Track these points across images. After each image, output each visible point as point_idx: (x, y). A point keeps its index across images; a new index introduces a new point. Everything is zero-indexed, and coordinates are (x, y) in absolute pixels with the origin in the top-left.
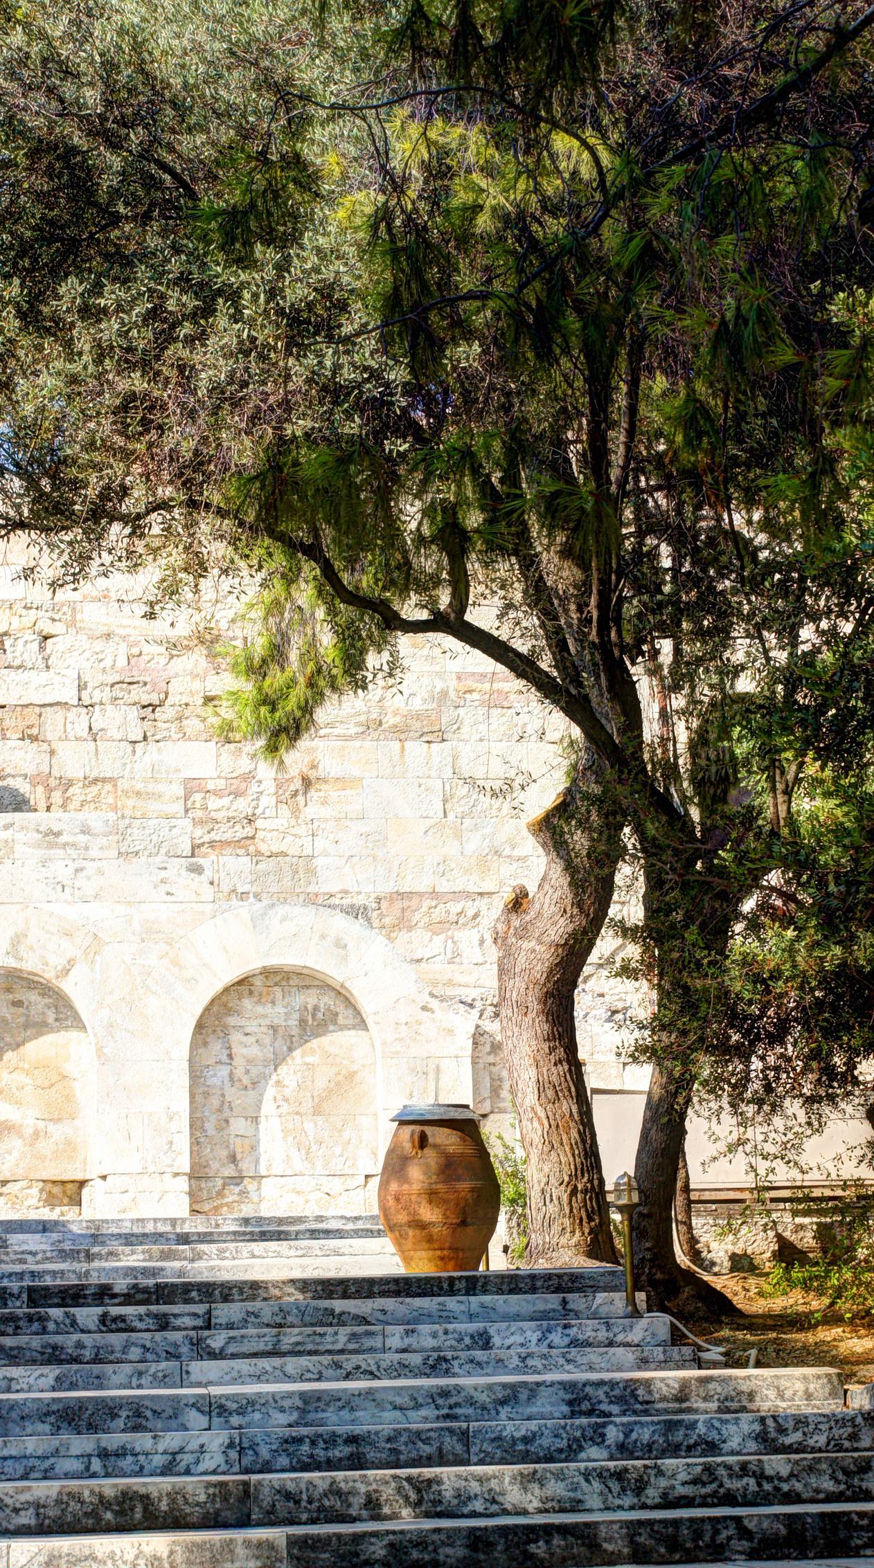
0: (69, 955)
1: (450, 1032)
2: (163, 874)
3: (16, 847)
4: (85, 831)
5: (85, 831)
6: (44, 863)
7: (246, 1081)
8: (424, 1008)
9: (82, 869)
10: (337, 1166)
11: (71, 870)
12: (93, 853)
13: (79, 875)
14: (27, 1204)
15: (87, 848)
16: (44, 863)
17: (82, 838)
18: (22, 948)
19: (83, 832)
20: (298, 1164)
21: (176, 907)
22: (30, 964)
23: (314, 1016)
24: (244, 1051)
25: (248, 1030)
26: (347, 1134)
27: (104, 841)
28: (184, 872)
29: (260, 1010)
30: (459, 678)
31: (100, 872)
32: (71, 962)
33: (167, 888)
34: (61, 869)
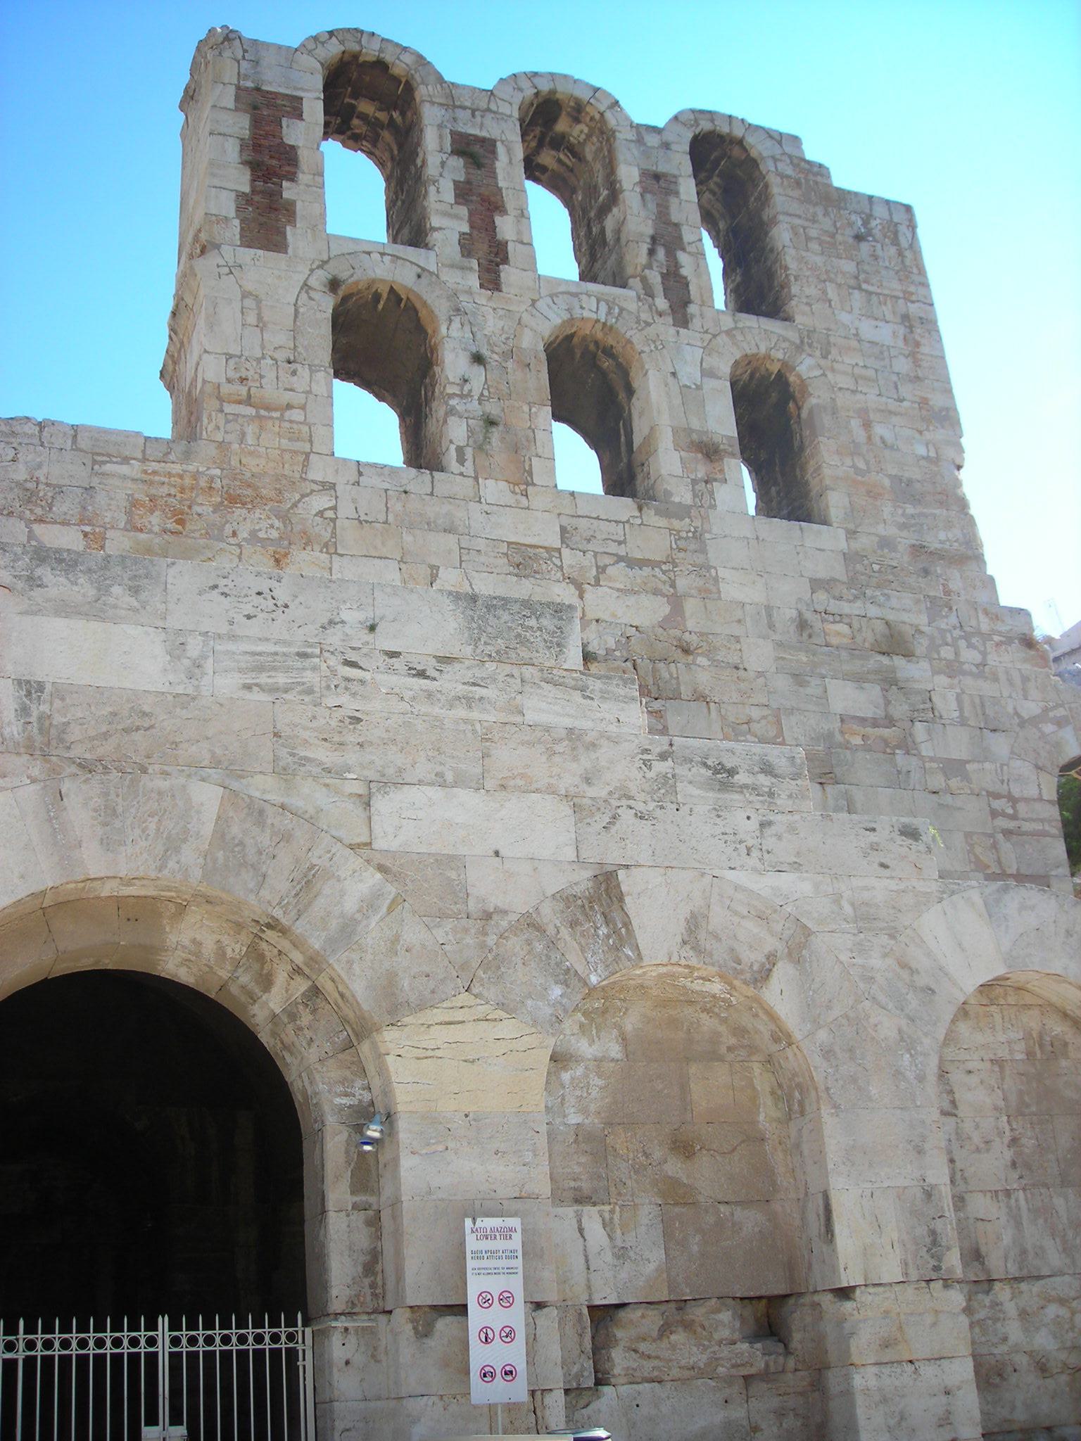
0: (768, 949)
2: (872, 837)
4: (767, 769)
5: (767, 769)
6: (718, 811)
9: (770, 823)
11: (753, 825)
12: (783, 801)
13: (768, 831)
16: (718, 811)
17: (764, 780)
18: (702, 935)
19: (763, 771)
21: (893, 885)
23: (1041, 1046)
25: (970, 1066)
28: (896, 835)
29: (980, 1038)
30: (842, 721)
31: (792, 829)
32: (772, 959)
33: (877, 857)
34: (742, 820)
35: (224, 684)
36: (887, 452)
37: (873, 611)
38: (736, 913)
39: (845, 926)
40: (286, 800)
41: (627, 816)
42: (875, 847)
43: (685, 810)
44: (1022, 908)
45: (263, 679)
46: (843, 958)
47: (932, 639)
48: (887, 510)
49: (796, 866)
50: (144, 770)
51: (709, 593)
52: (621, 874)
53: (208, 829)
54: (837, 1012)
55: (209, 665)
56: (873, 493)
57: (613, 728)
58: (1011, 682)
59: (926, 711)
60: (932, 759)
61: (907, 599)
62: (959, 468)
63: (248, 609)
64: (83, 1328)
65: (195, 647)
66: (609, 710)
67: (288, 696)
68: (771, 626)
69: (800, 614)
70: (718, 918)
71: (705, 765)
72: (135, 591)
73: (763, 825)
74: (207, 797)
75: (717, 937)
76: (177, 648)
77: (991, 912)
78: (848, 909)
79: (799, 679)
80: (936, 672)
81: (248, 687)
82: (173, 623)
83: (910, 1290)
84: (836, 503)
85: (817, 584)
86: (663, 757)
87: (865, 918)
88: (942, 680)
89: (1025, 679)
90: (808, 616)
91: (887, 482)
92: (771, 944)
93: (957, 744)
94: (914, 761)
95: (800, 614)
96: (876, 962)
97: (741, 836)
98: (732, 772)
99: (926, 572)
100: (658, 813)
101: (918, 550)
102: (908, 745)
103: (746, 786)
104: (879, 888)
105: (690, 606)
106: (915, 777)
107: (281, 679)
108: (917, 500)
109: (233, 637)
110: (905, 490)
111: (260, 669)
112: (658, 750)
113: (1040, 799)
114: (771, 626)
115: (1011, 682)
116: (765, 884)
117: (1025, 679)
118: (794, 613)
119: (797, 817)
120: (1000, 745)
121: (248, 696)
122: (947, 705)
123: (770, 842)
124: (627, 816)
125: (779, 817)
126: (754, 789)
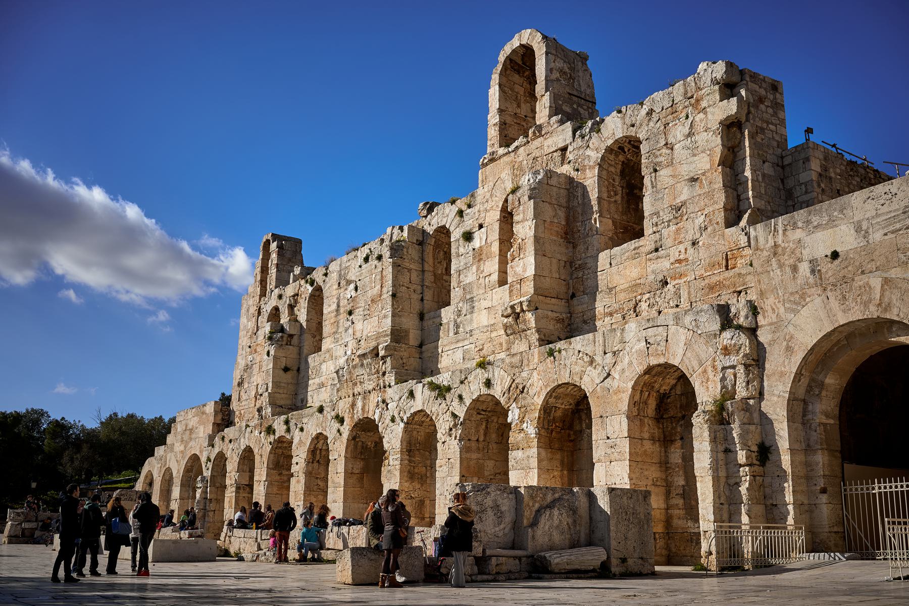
35: (877, 236)
40: (905, 276)
45: (891, 228)
50: (853, 280)
53: (878, 297)
55: (870, 231)
63: (883, 201)
64: (862, 484)
65: (865, 226)
67: (901, 232)
72: (841, 211)
74: (876, 282)
76: (858, 229)
81: (886, 234)
82: (856, 219)
107: (898, 226)
109: (877, 215)
111: (889, 225)
121: (886, 237)
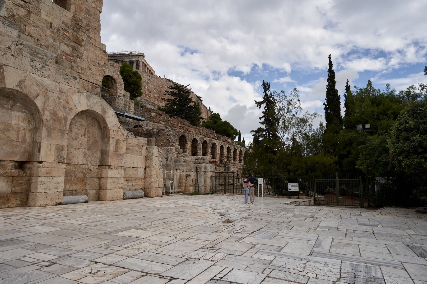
1: (123, 134)
2: (67, 77)
3: (24, 52)
7: (74, 138)
8: (119, 128)
9: (44, 67)
10: (93, 163)
11: (41, 66)
13: (43, 69)
14: (8, 168)
15: (46, 61)
16: (33, 61)
17: (45, 57)
19: (46, 56)
20: (85, 162)
21: (69, 87)
22: (25, 91)
24: (74, 130)
25: (76, 125)
26: (95, 155)
27: (51, 61)
29: (79, 120)
31: (49, 70)
33: (67, 81)
36: (86, 3)
37: (75, 33)
38: (32, 83)
39: (57, 92)
41: (9, 55)
42: (66, 79)
43: (24, 58)
44: (94, 98)
46: (55, 98)
47: (85, 43)
48: (83, 14)
49: (48, 77)
51: (38, 14)
52: (4, 67)
54: (51, 108)
56: (81, 9)
57: (9, 34)
58: (99, 58)
59: (81, 56)
60: (80, 66)
61: (82, 34)
62: (100, 13)
66: (9, 29)
68: (51, 27)
69: (58, 27)
70: (27, 82)
71: (32, 50)
73: (43, 67)
75: (26, 86)
77: (88, 97)
78: (58, 90)
79: (54, 40)
80: (85, 50)
83: (55, 164)
84: (72, 8)
85: (63, 23)
86: (21, 44)
87: (61, 91)
88: (85, 52)
89: (102, 58)
90: (60, 28)
91: (84, 9)
92: (39, 91)
93: (85, 65)
94: (75, 66)
95: (58, 27)
96: (62, 101)
97: (37, 67)
98: (38, 53)
99: (88, 30)
100: (17, 56)
101: (87, 25)
102: (75, 62)
103: (40, 57)
104: (65, 87)
105: (32, 15)
106: (75, 68)
108: (90, 15)
110: (88, 12)
112: (20, 42)
113: (99, 80)
114: (51, 27)
115: (99, 58)
116: (40, 79)
117: (102, 58)
118: (57, 27)
119: (51, 67)
120: (93, 68)
122: (85, 57)
123: (43, 71)
124: (9, 55)
125: (47, 66)
126: (42, 59)
